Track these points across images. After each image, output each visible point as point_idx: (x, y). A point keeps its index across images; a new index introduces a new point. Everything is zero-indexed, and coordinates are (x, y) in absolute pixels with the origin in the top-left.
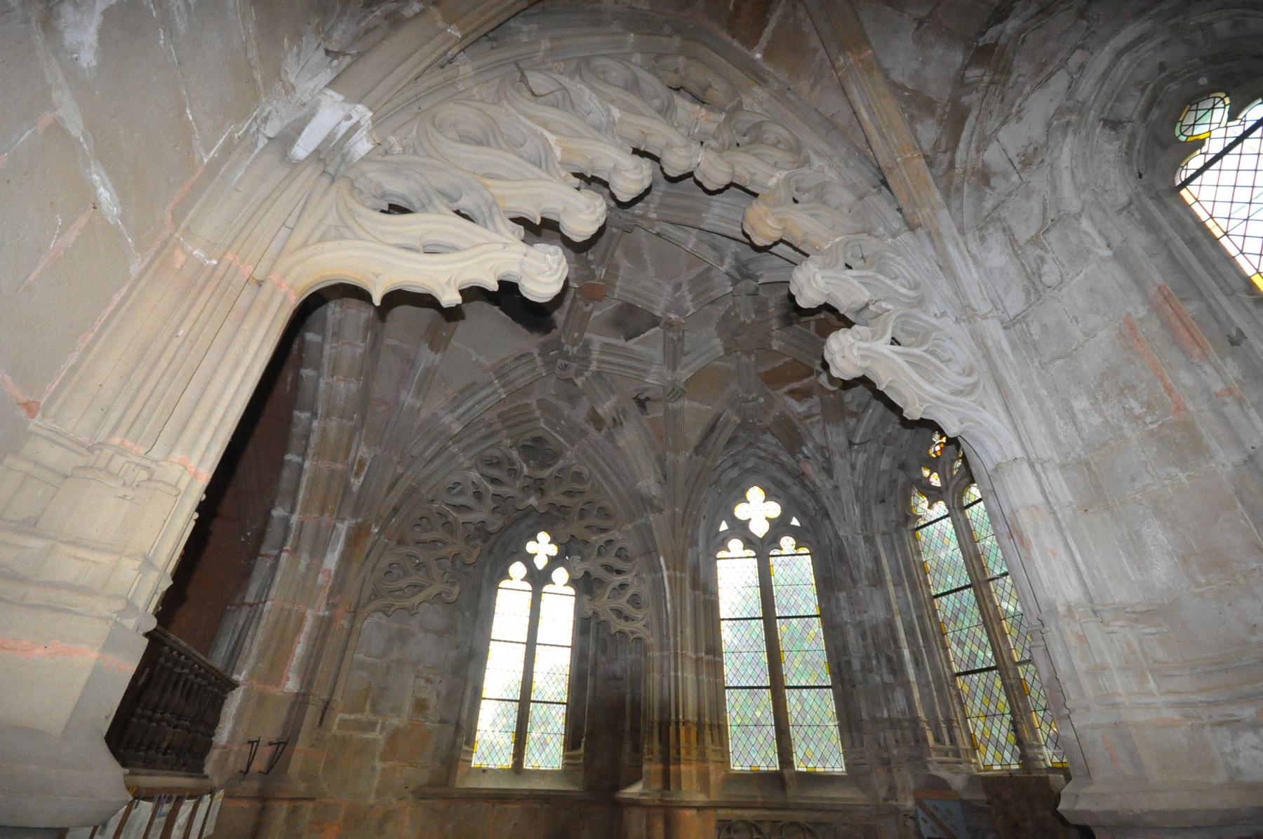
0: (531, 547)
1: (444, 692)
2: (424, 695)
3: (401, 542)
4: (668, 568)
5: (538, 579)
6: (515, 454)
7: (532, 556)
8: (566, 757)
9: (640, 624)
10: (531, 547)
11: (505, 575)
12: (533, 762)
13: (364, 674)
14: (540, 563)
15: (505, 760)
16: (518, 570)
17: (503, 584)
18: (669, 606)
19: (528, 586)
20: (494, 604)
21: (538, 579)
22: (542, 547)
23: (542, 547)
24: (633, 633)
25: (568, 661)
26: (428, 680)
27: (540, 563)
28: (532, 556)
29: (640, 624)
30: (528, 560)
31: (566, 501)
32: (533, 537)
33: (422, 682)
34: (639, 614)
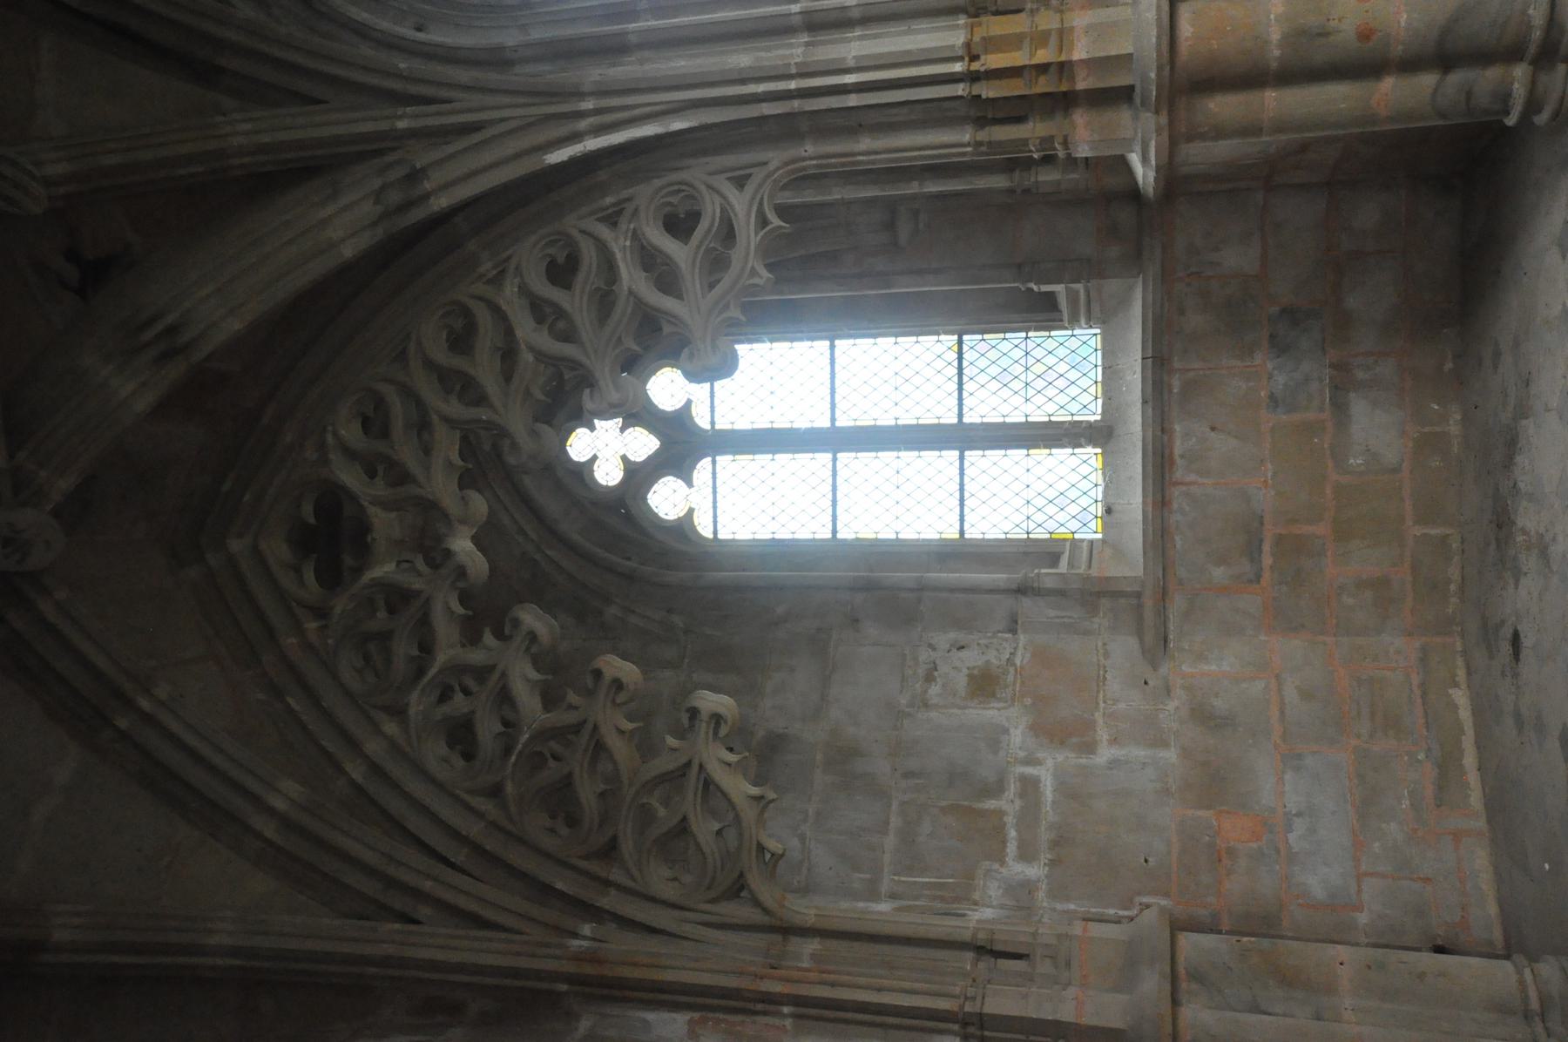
0: (608, 474)
1: (952, 635)
2: (961, 682)
3: (610, 851)
4: (576, 137)
5: (682, 445)
6: (341, 605)
7: (631, 469)
8: (1074, 322)
9: (740, 203)
10: (608, 474)
11: (683, 527)
12: (1086, 399)
13: (926, 827)
14: (642, 444)
15: (1085, 463)
16: (666, 499)
17: (704, 528)
18: (678, 125)
19: (703, 469)
20: (755, 543)
21: (682, 445)
22: (603, 448)
23: (603, 448)
24: (763, 222)
25: (804, 534)
26: (929, 678)
27: (642, 444)
28: (631, 469)
29: (740, 203)
30: (639, 476)
31: (447, 447)
32: (582, 472)
33: (934, 690)
34: (711, 210)
